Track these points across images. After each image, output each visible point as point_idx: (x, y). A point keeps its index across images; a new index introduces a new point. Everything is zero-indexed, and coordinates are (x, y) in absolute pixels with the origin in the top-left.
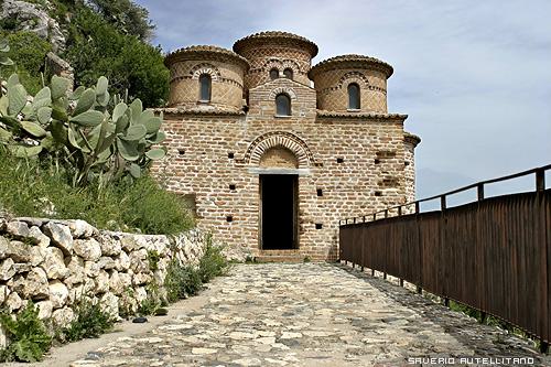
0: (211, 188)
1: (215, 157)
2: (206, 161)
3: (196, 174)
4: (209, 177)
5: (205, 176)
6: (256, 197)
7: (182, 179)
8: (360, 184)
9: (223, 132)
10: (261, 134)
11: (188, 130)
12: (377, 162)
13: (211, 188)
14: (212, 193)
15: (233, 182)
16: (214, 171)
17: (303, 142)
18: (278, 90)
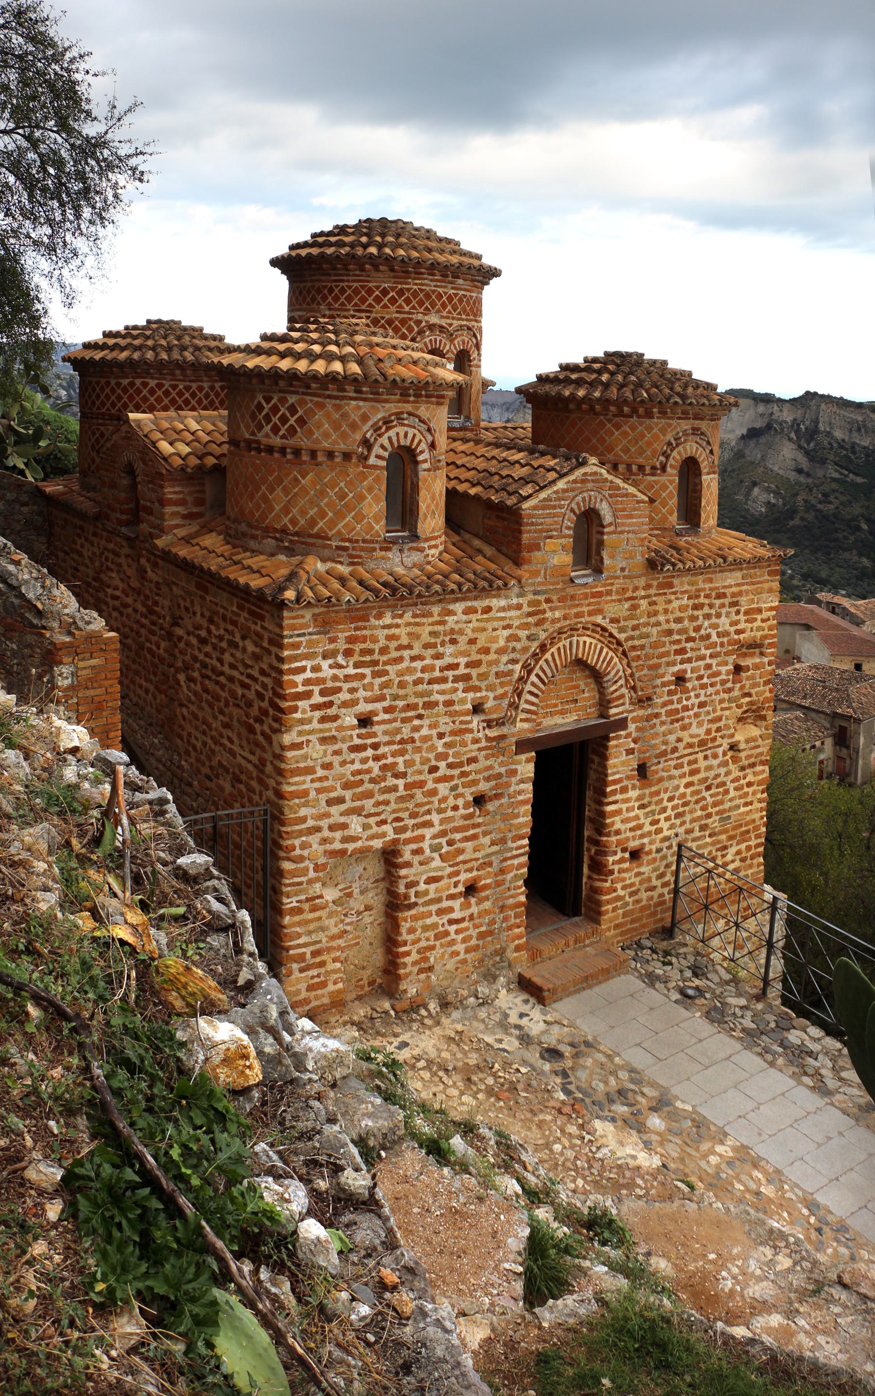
0: (435, 818)
1: (445, 724)
2: (426, 739)
3: (401, 783)
4: (430, 785)
5: (421, 784)
6: (524, 818)
7: (368, 804)
8: (708, 732)
9: (463, 640)
10: (543, 635)
11: (384, 650)
12: (738, 669)
13: (435, 818)
14: (437, 828)
15: (484, 787)
16: (442, 764)
17: (619, 643)
18: (579, 502)
